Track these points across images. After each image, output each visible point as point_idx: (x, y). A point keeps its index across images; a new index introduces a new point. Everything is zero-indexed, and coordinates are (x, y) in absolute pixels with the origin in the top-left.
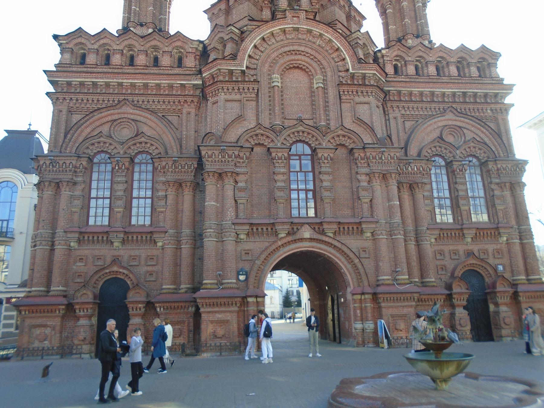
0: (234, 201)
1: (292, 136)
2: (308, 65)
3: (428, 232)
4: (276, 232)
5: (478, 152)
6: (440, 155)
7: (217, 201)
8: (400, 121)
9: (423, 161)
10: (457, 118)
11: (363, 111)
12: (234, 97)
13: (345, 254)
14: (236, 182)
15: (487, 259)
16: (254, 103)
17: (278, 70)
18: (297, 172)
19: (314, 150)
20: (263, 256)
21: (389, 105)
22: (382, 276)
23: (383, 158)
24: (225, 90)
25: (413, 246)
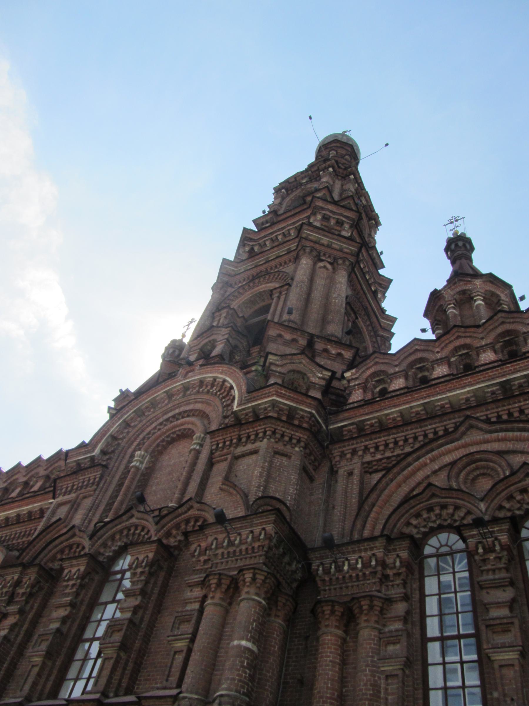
10: (488, 436)
21: (336, 453)
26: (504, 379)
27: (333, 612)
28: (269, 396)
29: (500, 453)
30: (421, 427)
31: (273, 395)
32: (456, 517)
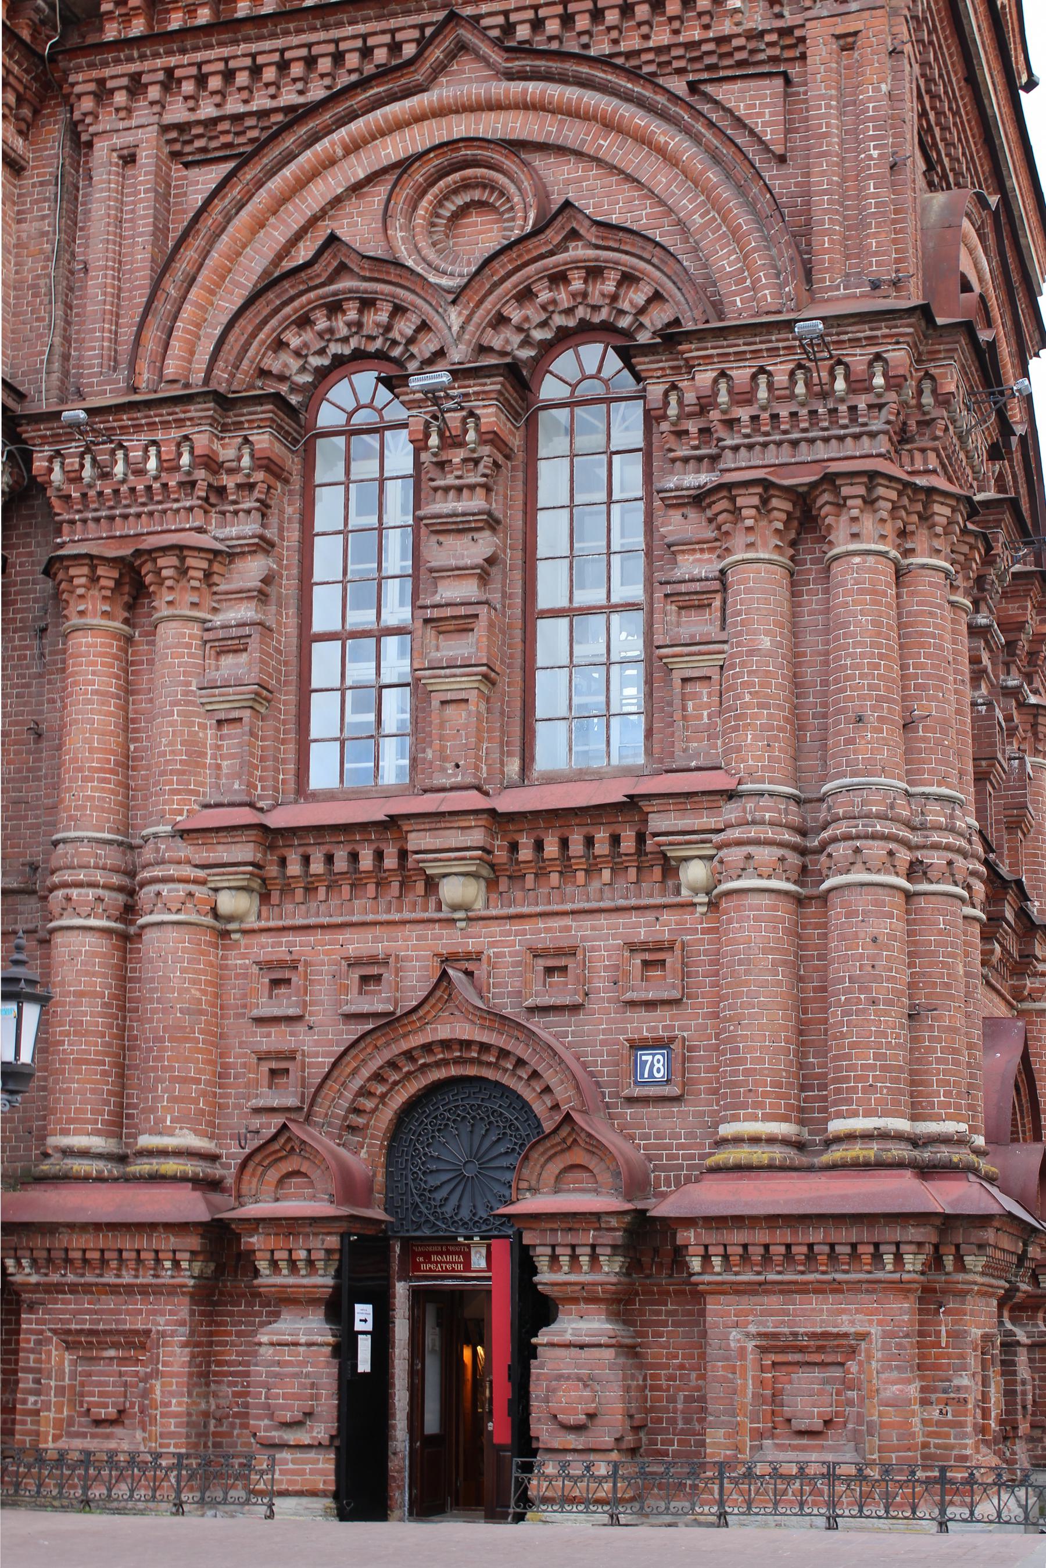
3: (184, 850)
10: (501, 89)
21: (81, 81)
27: (94, 579)
30: (326, 27)
32: (395, 334)
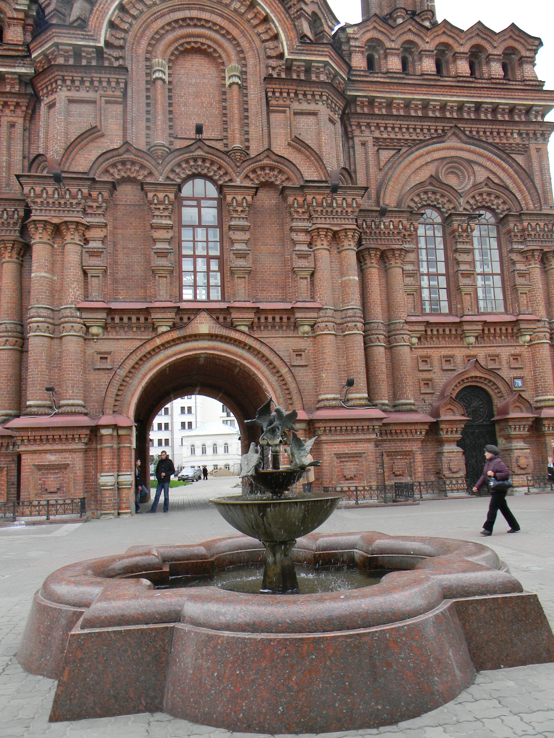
0: (80, 273)
1: (184, 165)
2: (214, 46)
3: (407, 327)
4: (153, 324)
5: (495, 202)
6: (434, 206)
7: (52, 272)
8: (371, 149)
9: (404, 215)
11: (306, 128)
12: (83, 94)
13: (267, 360)
14: (87, 241)
15: (499, 369)
16: (119, 108)
17: (165, 52)
18: (194, 227)
19: (220, 189)
20: (131, 362)
21: (354, 121)
22: (325, 394)
23: (335, 205)
24: (69, 83)
25: (382, 350)
26: (480, 100)
28: (322, 55)
29: (470, 162)
30: (421, 122)
31: (326, 55)
